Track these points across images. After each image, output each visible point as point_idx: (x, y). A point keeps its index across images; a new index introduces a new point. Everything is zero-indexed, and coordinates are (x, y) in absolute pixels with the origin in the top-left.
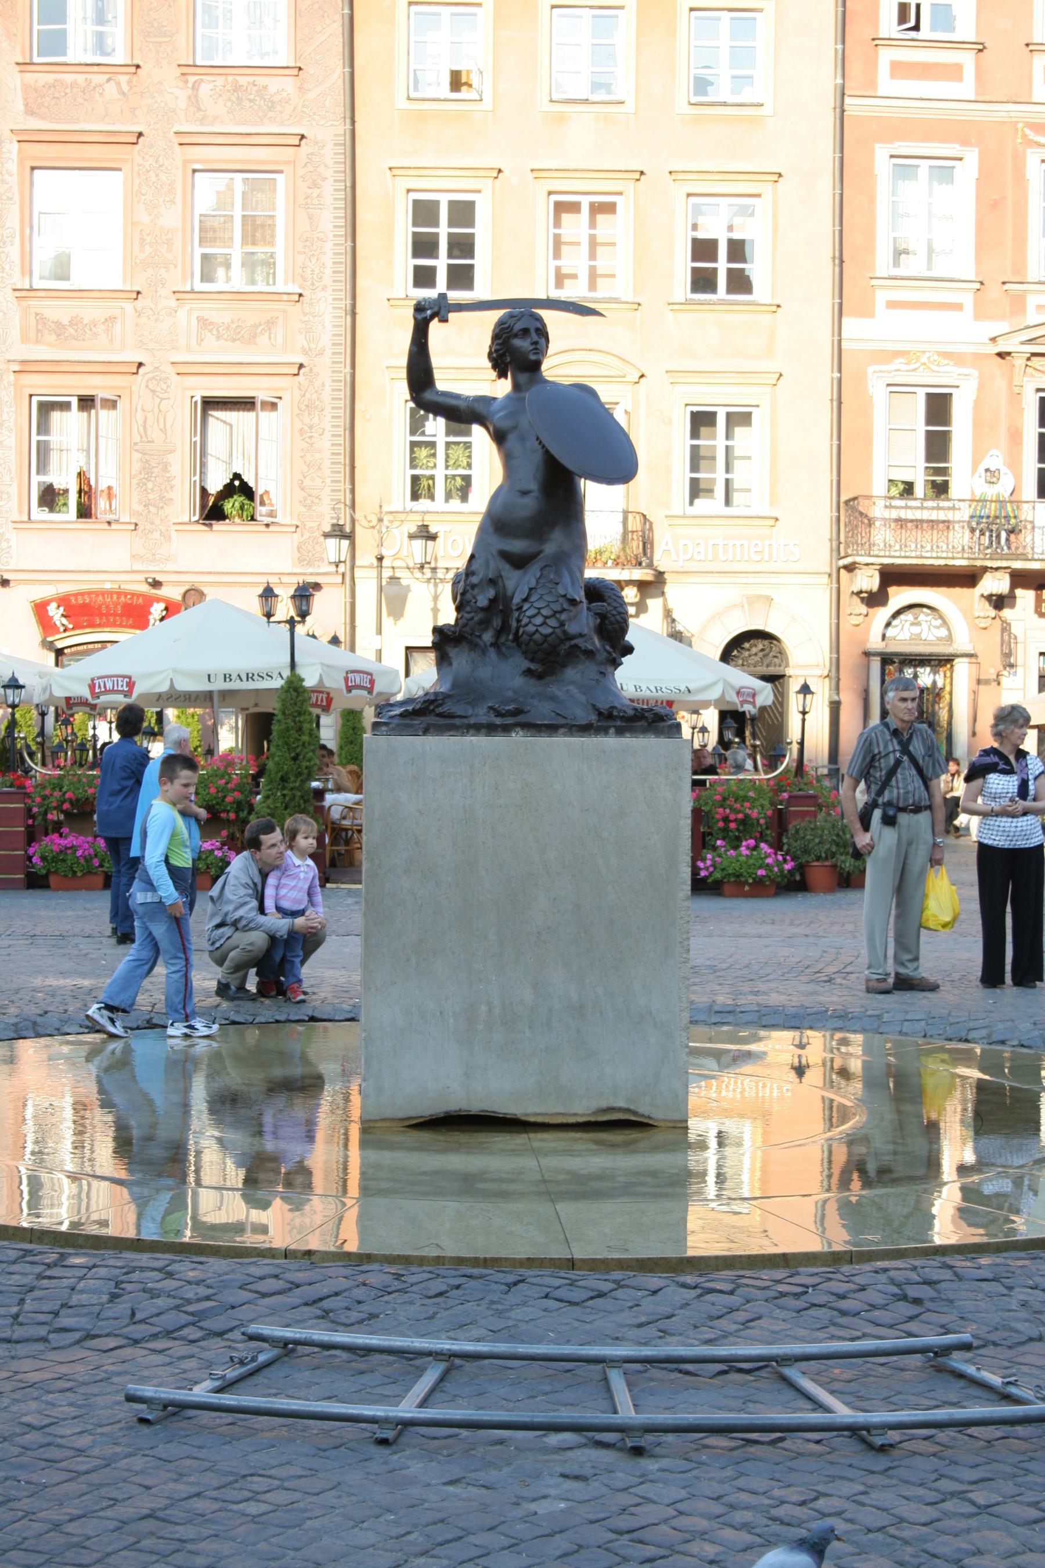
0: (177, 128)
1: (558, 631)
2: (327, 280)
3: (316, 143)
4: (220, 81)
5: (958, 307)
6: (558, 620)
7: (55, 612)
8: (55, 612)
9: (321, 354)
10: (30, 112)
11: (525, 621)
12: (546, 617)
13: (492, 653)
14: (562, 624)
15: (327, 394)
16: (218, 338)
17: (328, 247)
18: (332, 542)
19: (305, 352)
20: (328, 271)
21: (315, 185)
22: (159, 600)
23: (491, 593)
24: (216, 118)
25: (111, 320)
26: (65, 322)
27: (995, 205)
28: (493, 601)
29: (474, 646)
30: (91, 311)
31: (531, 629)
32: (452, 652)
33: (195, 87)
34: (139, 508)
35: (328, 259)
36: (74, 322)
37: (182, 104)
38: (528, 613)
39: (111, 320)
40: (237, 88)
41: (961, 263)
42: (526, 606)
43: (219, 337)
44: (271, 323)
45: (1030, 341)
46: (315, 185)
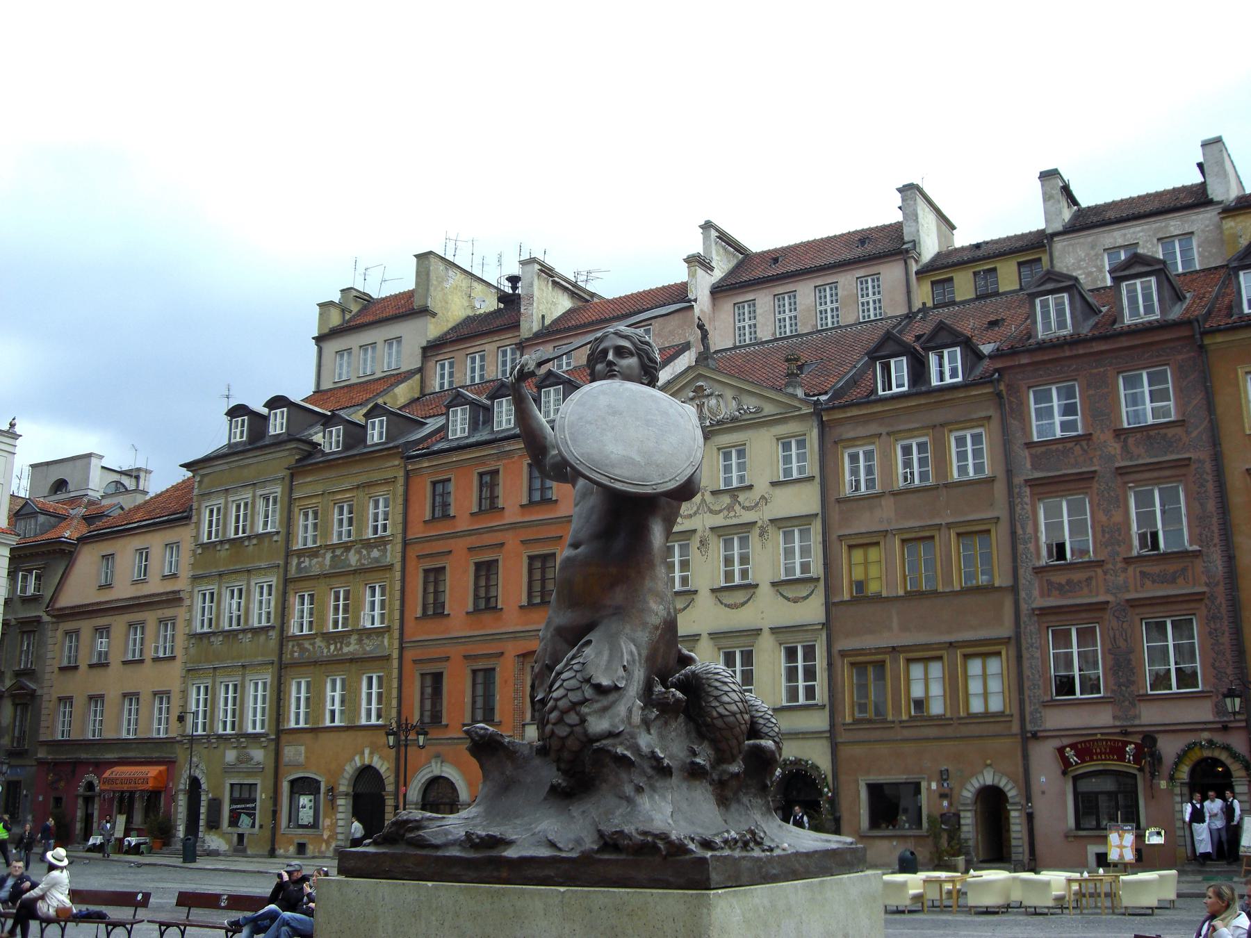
0: (1117, 465)
2: (1216, 541)
3: (1199, 461)
4: (1139, 435)
7: (1069, 752)
8: (1069, 752)
9: (1217, 584)
10: (1035, 467)
15: (1224, 609)
16: (1154, 582)
17: (1215, 520)
18: (1228, 701)
19: (1207, 585)
20: (1216, 535)
21: (1202, 485)
22: (1131, 743)
24: (1139, 456)
25: (1089, 579)
26: (1063, 582)
30: (1077, 576)
33: (1125, 441)
34: (1115, 688)
35: (1215, 529)
36: (1069, 582)
37: (1118, 451)
39: (1089, 579)
40: (1149, 437)
43: (1154, 582)
44: (1184, 570)
46: (1202, 485)
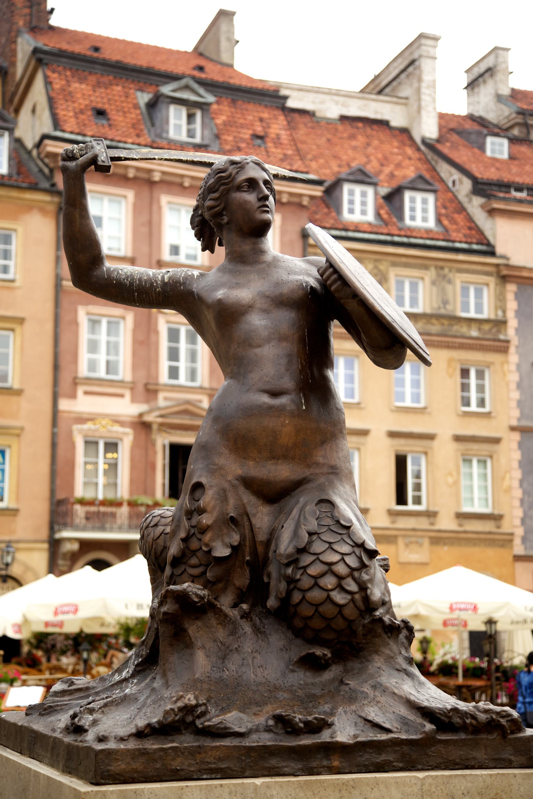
1: (357, 597)
5: (122, 396)
6: (354, 579)
11: (306, 582)
12: (340, 578)
13: (247, 628)
14: (363, 588)
23: (235, 539)
27: (142, 343)
28: (236, 549)
29: (223, 618)
31: (316, 595)
32: (194, 629)
38: (313, 571)
41: (124, 372)
42: (306, 559)
45: (162, 416)
